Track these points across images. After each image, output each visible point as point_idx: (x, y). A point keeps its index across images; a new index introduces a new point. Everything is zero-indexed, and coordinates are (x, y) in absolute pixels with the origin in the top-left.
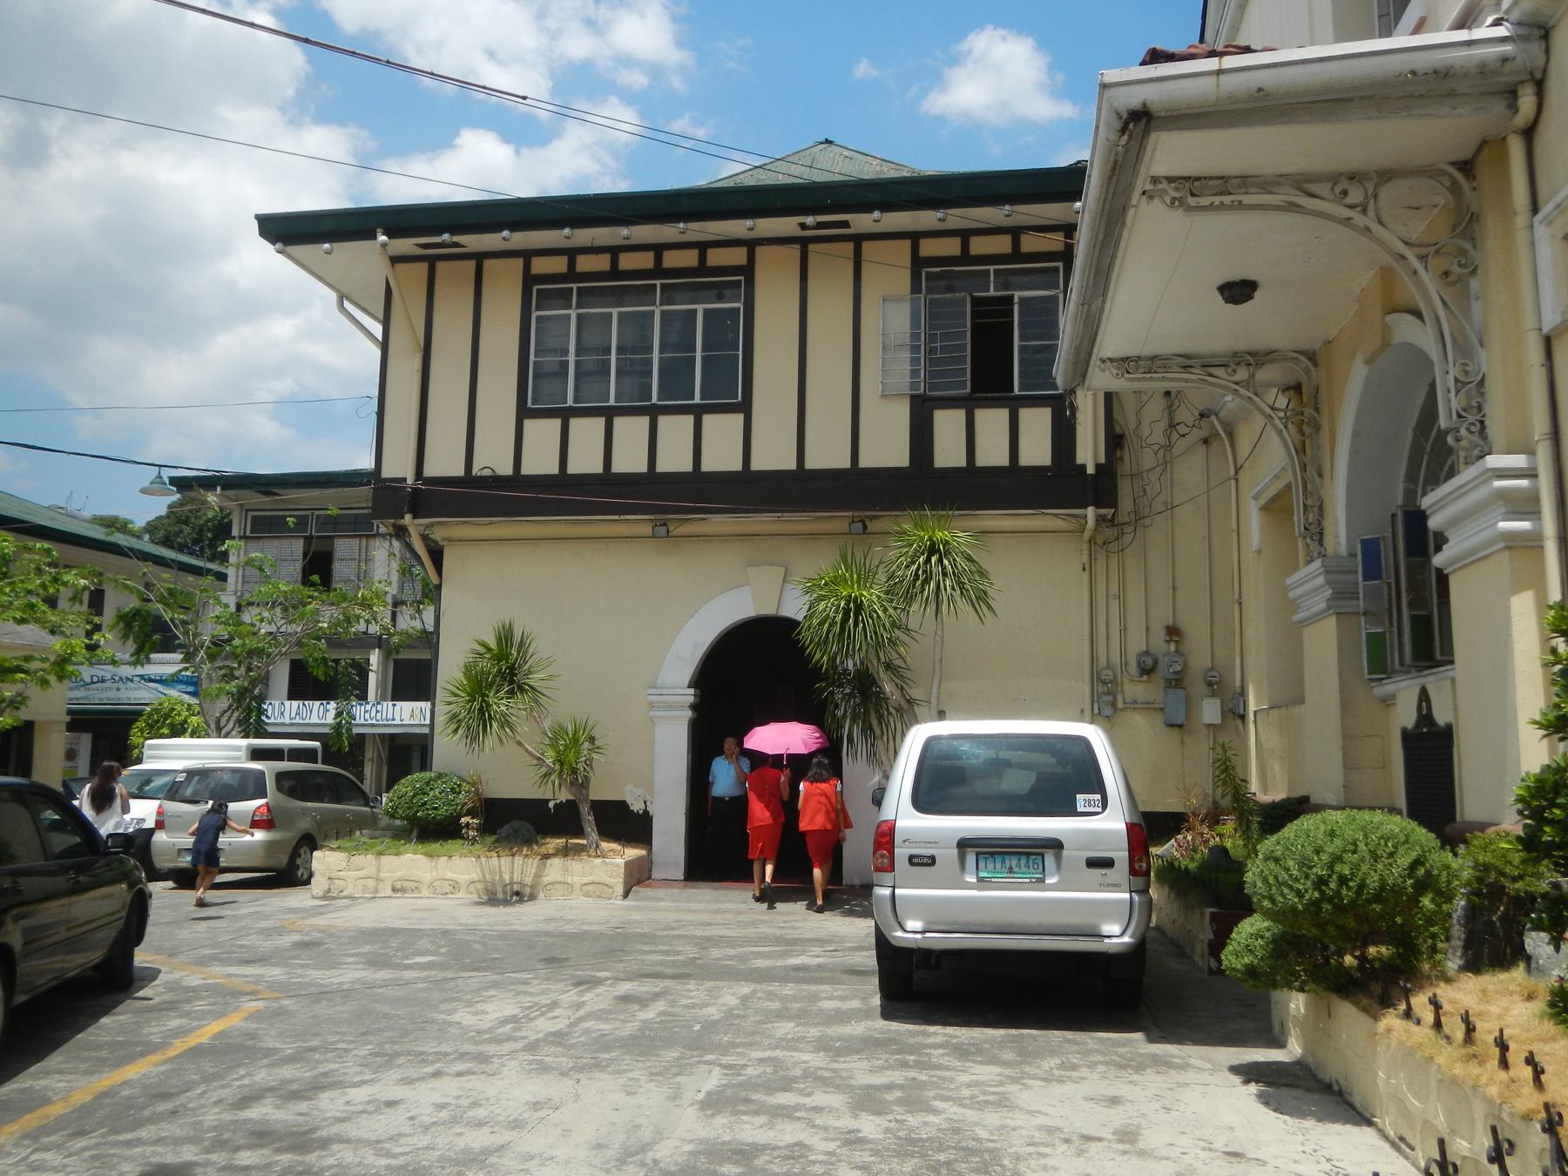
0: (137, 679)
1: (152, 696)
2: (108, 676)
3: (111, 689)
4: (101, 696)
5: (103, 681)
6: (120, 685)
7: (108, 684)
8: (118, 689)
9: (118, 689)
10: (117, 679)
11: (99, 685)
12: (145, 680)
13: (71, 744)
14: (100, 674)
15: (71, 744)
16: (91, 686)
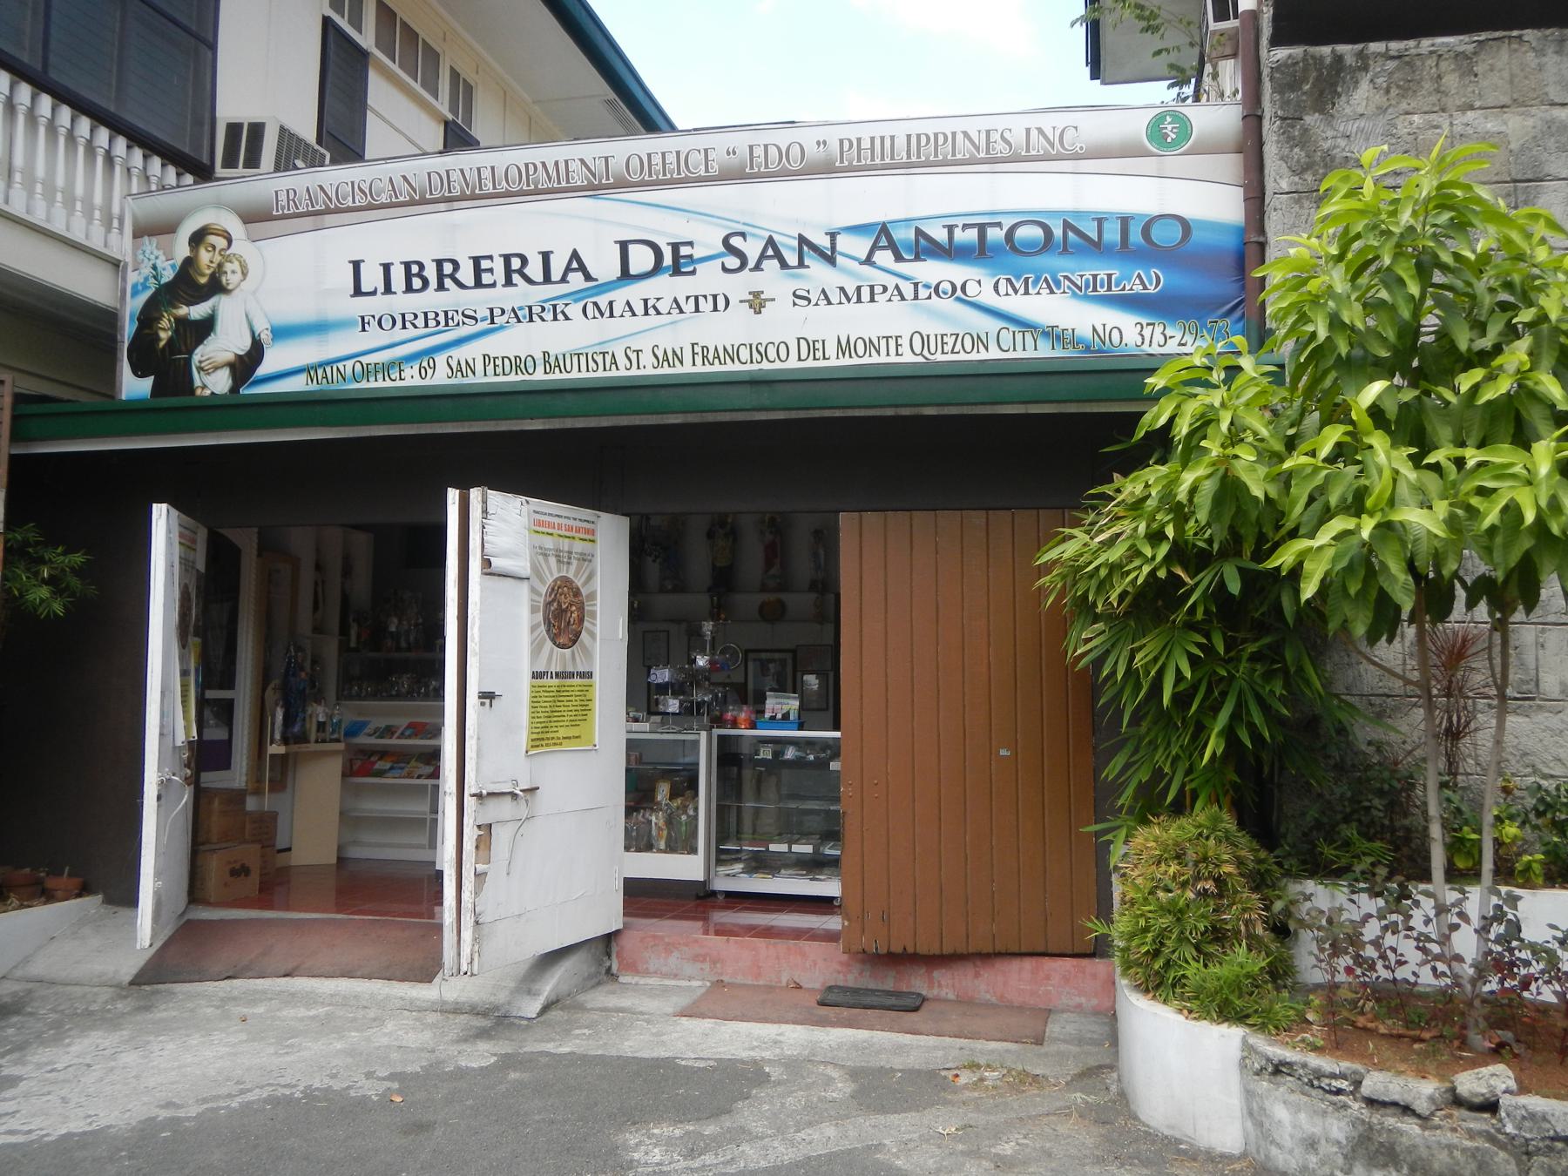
0: (861, 246)
1: (931, 328)
2: (707, 240)
3: (720, 303)
4: (667, 342)
5: (680, 264)
6: (771, 279)
7: (708, 279)
8: (757, 303)
9: (757, 303)
10: (752, 249)
11: (665, 287)
12: (892, 246)
13: (562, 558)
14: (666, 230)
15: (562, 558)
16: (620, 296)
